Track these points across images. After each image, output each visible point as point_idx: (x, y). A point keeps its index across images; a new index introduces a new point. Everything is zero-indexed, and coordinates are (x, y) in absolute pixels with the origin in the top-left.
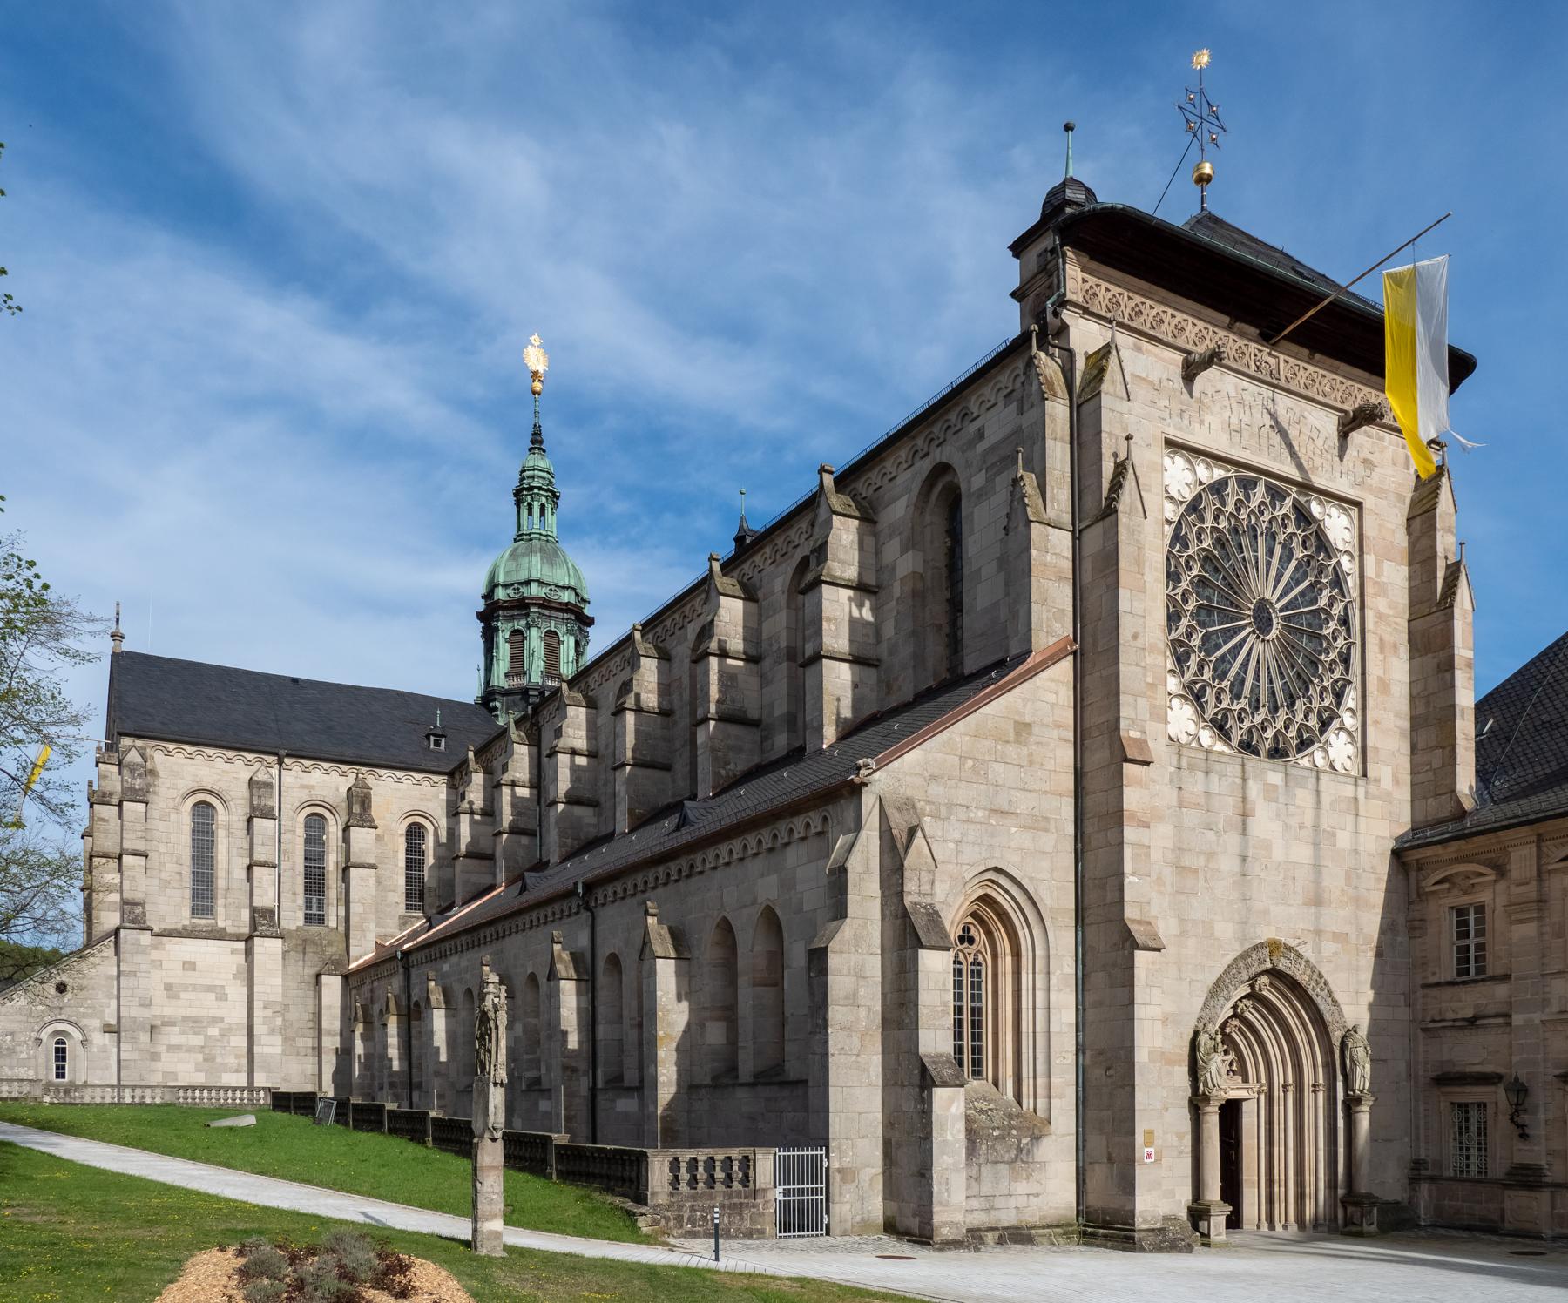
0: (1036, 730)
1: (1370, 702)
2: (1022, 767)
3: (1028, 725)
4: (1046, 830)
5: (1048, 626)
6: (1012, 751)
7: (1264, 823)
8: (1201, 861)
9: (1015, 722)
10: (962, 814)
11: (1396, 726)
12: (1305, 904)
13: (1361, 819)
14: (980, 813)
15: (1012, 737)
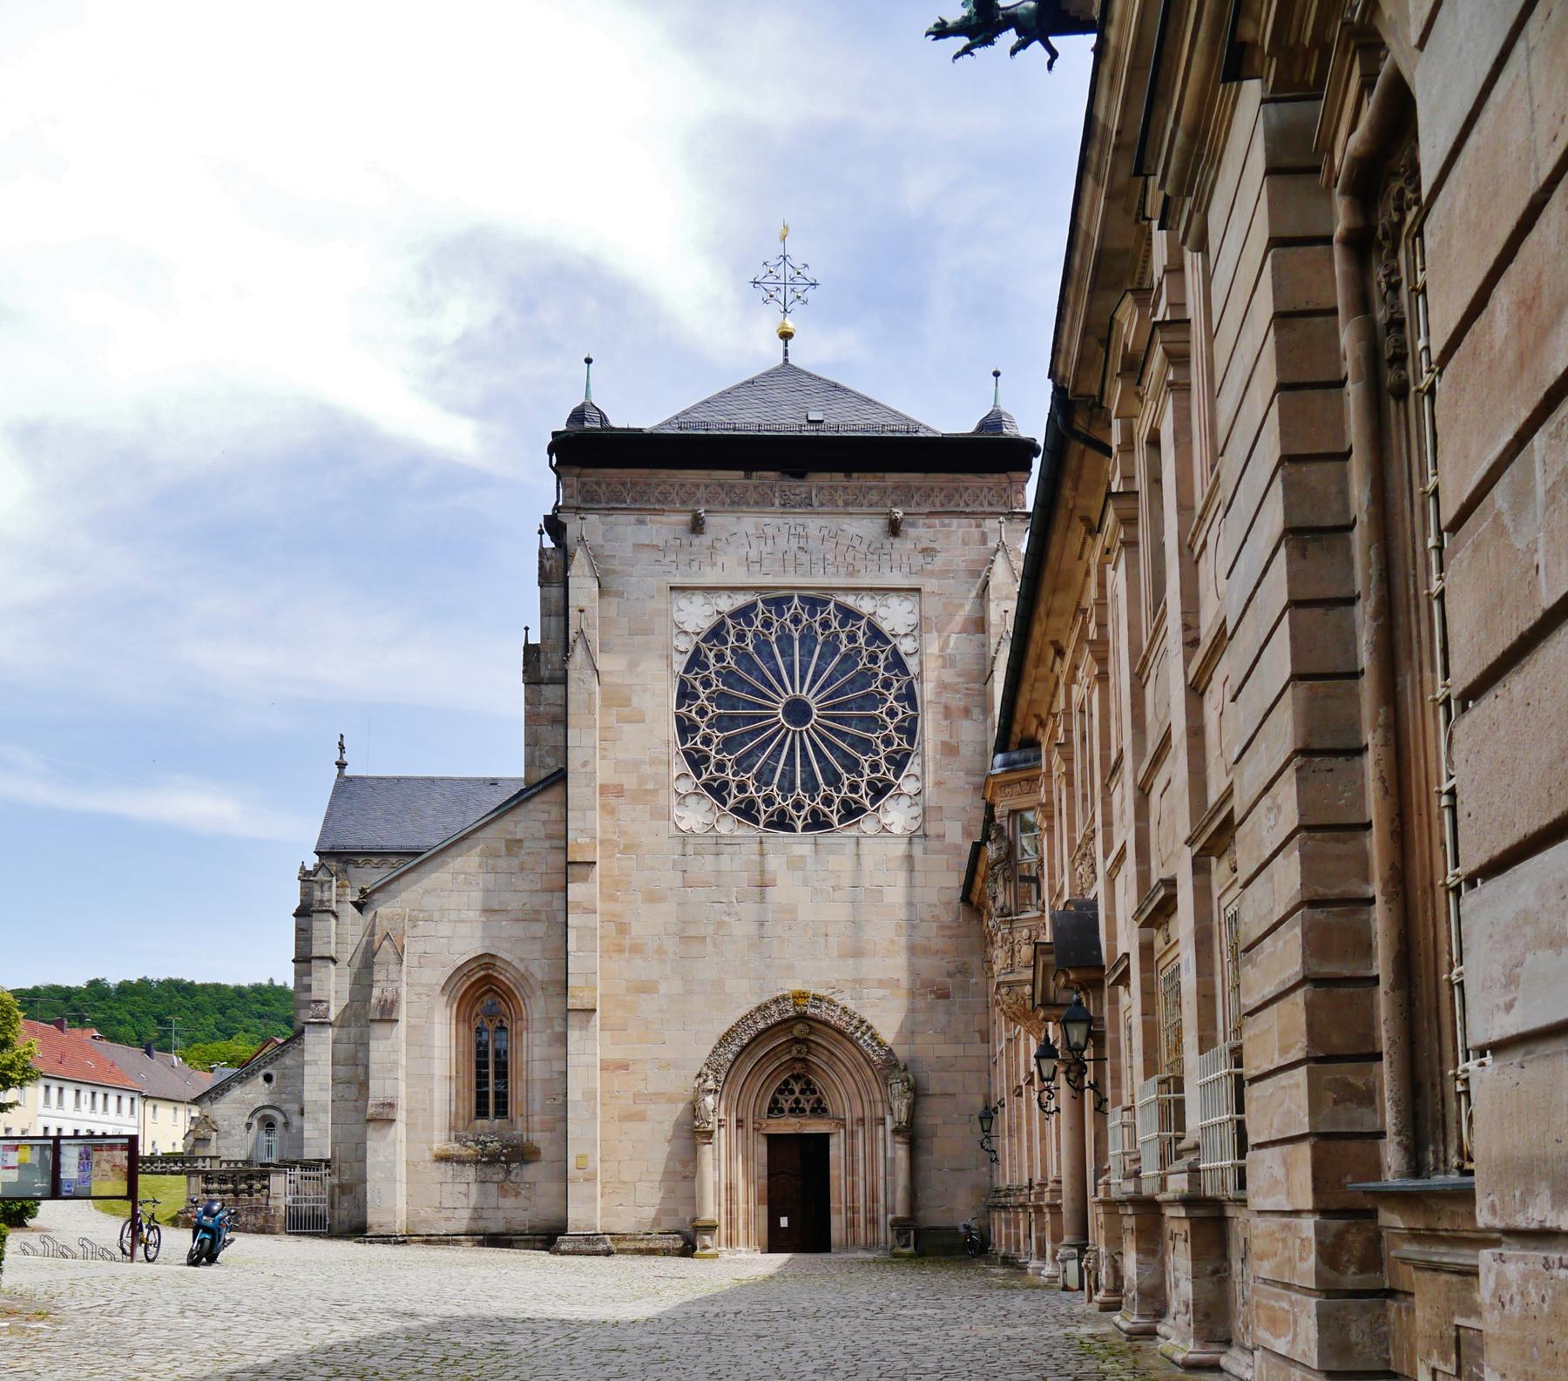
0: (526, 844)
1: (930, 766)
2: (512, 874)
3: (520, 841)
4: (537, 920)
5: (541, 762)
6: (502, 863)
7: (785, 890)
8: (710, 930)
9: (507, 840)
10: (453, 915)
11: (968, 783)
12: (840, 956)
13: (916, 874)
14: (471, 914)
15: (503, 850)
